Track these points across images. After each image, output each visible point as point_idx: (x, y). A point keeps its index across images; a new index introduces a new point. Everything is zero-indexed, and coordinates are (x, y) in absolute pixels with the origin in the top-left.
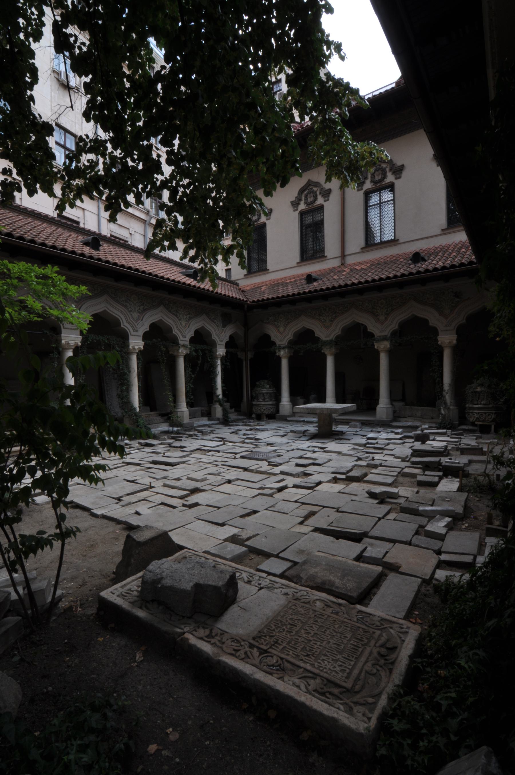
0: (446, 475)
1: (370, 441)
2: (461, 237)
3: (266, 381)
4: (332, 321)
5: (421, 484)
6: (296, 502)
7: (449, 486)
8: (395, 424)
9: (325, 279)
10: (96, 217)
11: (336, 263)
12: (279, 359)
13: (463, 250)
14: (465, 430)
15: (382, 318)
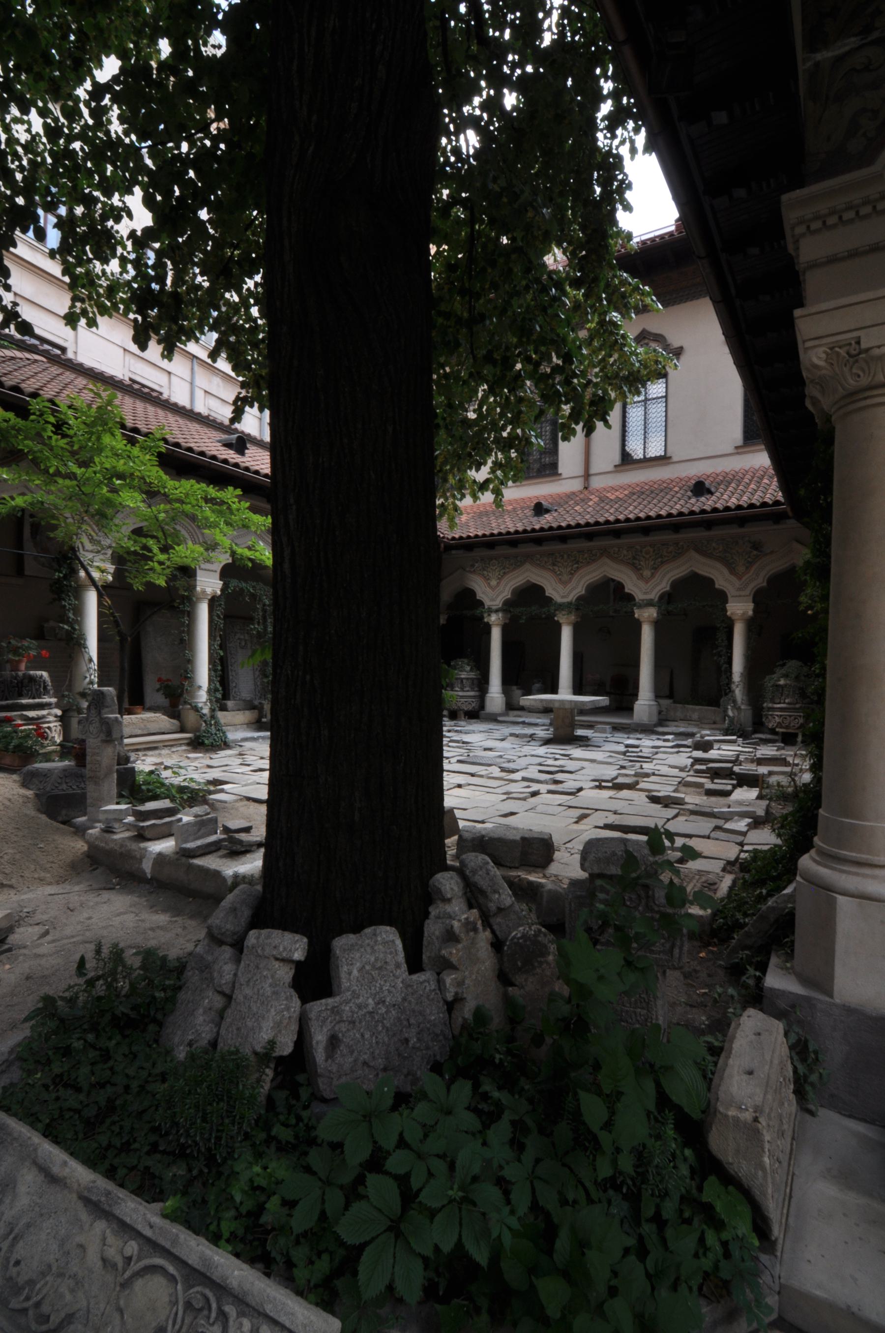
0: (740, 785)
1: (630, 749)
2: (761, 459)
3: (466, 661)
4: (572, 574)
5: (710, 793)
6: (559, 805)
7: (746, 795)
8: (660, 729)
9: (561, 510)
10: (187, 386)
11: (576, 485)
12: (488, 628)
13: (766, 481)
14: (761, 739)
15: (647, 573)
